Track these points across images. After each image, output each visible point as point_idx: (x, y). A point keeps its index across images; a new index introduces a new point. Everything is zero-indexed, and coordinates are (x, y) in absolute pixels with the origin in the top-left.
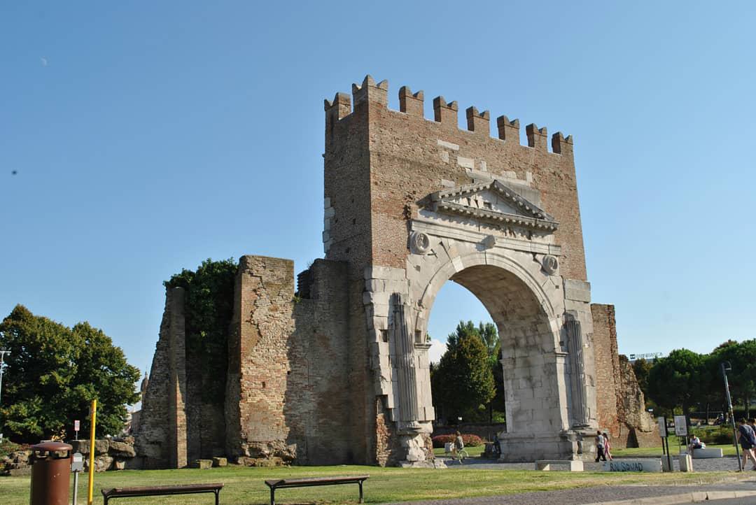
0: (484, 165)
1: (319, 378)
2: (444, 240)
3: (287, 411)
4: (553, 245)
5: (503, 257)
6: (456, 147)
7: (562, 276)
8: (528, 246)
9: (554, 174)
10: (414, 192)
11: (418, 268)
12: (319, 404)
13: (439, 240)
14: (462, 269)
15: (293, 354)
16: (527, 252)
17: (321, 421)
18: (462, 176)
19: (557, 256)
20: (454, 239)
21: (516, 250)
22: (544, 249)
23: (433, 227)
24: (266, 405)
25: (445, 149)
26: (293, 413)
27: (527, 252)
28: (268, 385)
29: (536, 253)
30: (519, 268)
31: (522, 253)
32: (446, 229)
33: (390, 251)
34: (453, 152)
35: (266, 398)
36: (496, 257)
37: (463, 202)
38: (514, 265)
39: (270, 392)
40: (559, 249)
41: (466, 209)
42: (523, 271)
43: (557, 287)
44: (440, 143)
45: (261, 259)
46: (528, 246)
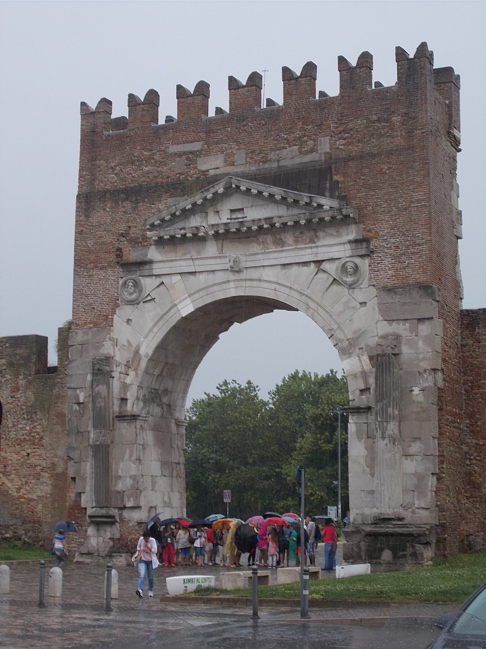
0: (240, 157)
1: (57, 459)
2: (165, 280)
3: (26, 494)
4: (350, 242)
5: (260, 280)
6: (197, 146)
7: (374, 285)
8: (307, 255)
9: (379, 121)
10: (130, 227)
11: (129, 321)
12: (53, 486)
13: (158, 281)
14: (193, 310)
15: (32, 434)
16: (306, 264)
17: (56, 505)
18: (207, 181)
19: (361, 256)
20: (180, 273)
21: (284, 265)
22: (337, 252)
23: (147, 267)
24: (7, 488)
25: (180, 155)
26: (30, 496)
27: (306, 264)
28: (8, 469)
29: (323, 261)
30: (288, 291)
31: (295, 268)
32: (167, 265)
33: (94, 308)
34: (191, 152)
35: (6, 482)
36: (248, 283)
37: (195, 221)
38: (278, 287)
39: (9, 475)
40: (365, 245)
41: (183, 232)
42: (295, 294)
43: (363, 304)
44: (173, 149)
45: (4, 340)
46: (307, 254)
